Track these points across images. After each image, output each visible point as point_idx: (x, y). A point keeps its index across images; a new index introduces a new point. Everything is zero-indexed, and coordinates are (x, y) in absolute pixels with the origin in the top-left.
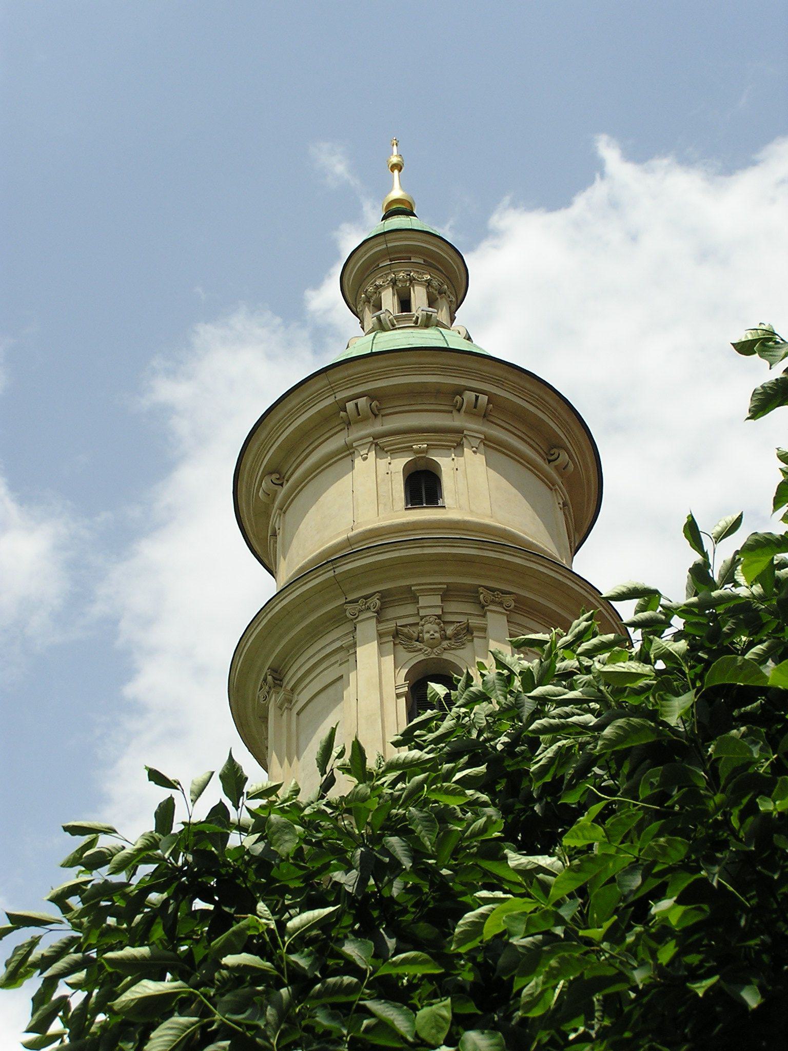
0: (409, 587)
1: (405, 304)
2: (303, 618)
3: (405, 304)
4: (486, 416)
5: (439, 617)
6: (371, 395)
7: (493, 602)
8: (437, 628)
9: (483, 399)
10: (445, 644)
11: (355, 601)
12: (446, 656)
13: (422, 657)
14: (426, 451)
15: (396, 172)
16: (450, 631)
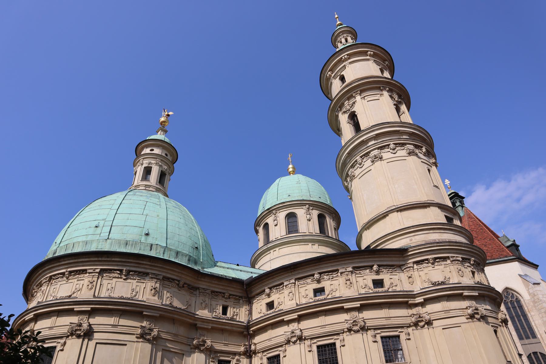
0: (342, 103)
1: (346, 41)
2: (333, 119)
3: (346, 41)
4: (349, 59)
5: (348, 104)
6: (329, 71)
7: (356, 95)
8: (348, 107)
9: (346, 56)
10: (351, 109)
11: (336, 111)
12: (352, 110)
13: (349, 113)
14: (340, 74)
15: (337, 18)
16: (351, 105)
